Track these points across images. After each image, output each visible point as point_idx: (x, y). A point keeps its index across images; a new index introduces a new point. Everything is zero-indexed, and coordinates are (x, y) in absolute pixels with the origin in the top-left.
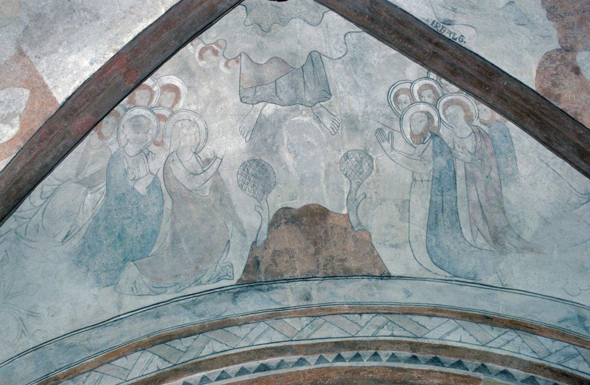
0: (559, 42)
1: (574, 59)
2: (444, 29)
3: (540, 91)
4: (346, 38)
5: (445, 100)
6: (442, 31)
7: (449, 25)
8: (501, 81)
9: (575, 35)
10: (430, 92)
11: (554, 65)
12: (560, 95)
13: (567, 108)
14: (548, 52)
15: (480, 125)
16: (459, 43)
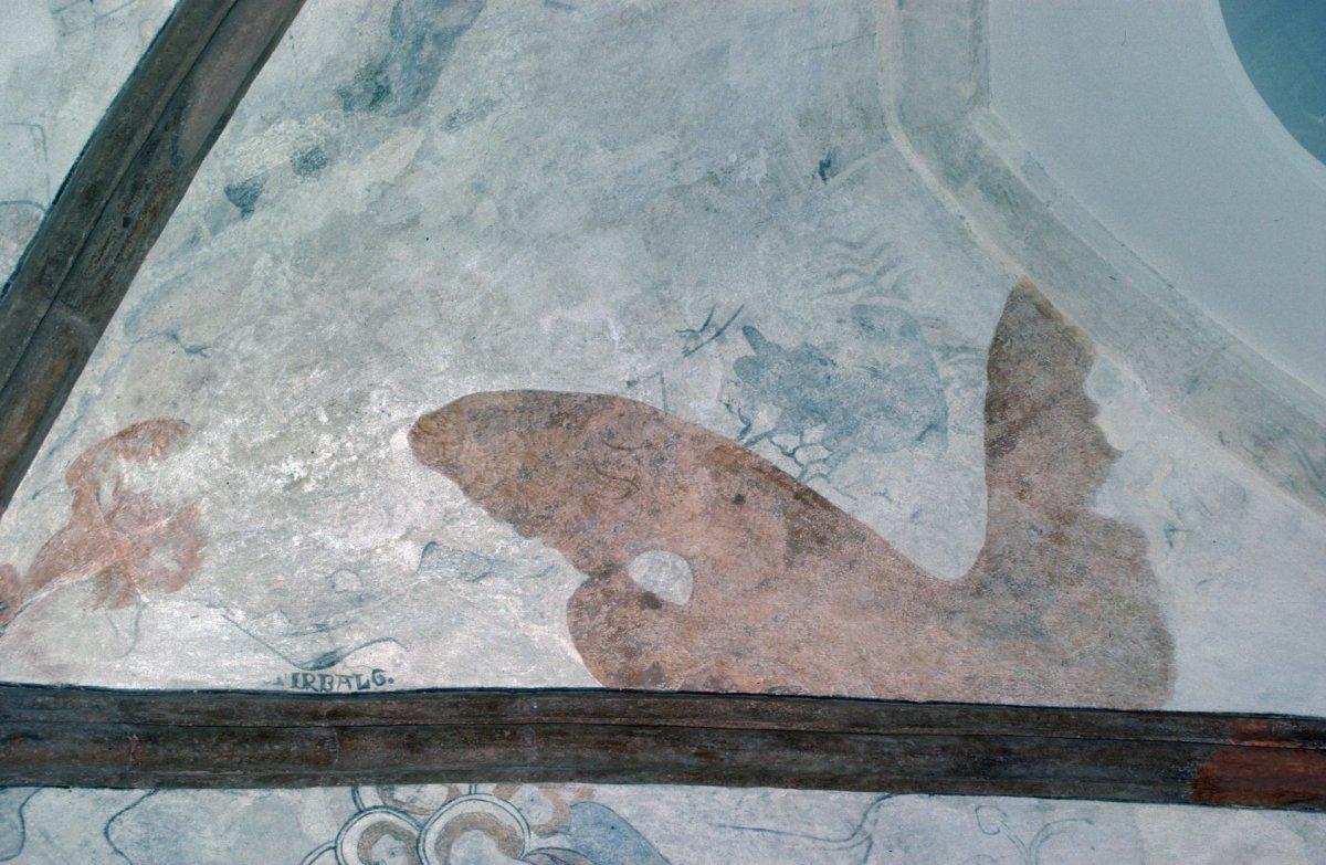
0: (578, 567)
1: (629, 583)
2: (328, 680)
3: (611, 683)
4: (112, 838)
5: (431, 837)
6: (328, 687)
7: (333, 664)
8: (522, 708)
9: (597, 537)
10: (387, 841)
11: (601, 618)
12: (656, 666)
13: (690, 682)
14: (571, 599)
15: (543, 843)
16: (380, 689)
